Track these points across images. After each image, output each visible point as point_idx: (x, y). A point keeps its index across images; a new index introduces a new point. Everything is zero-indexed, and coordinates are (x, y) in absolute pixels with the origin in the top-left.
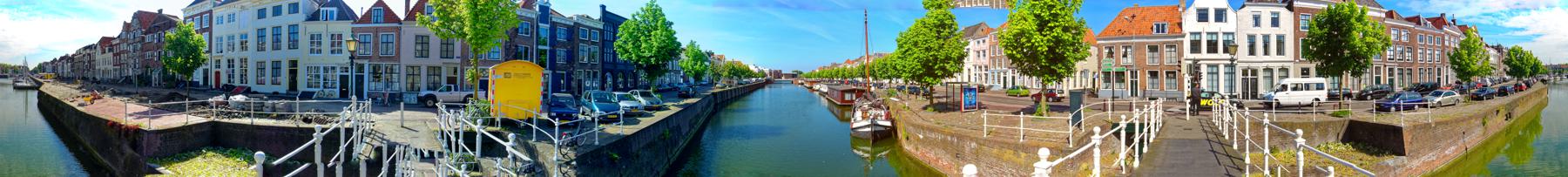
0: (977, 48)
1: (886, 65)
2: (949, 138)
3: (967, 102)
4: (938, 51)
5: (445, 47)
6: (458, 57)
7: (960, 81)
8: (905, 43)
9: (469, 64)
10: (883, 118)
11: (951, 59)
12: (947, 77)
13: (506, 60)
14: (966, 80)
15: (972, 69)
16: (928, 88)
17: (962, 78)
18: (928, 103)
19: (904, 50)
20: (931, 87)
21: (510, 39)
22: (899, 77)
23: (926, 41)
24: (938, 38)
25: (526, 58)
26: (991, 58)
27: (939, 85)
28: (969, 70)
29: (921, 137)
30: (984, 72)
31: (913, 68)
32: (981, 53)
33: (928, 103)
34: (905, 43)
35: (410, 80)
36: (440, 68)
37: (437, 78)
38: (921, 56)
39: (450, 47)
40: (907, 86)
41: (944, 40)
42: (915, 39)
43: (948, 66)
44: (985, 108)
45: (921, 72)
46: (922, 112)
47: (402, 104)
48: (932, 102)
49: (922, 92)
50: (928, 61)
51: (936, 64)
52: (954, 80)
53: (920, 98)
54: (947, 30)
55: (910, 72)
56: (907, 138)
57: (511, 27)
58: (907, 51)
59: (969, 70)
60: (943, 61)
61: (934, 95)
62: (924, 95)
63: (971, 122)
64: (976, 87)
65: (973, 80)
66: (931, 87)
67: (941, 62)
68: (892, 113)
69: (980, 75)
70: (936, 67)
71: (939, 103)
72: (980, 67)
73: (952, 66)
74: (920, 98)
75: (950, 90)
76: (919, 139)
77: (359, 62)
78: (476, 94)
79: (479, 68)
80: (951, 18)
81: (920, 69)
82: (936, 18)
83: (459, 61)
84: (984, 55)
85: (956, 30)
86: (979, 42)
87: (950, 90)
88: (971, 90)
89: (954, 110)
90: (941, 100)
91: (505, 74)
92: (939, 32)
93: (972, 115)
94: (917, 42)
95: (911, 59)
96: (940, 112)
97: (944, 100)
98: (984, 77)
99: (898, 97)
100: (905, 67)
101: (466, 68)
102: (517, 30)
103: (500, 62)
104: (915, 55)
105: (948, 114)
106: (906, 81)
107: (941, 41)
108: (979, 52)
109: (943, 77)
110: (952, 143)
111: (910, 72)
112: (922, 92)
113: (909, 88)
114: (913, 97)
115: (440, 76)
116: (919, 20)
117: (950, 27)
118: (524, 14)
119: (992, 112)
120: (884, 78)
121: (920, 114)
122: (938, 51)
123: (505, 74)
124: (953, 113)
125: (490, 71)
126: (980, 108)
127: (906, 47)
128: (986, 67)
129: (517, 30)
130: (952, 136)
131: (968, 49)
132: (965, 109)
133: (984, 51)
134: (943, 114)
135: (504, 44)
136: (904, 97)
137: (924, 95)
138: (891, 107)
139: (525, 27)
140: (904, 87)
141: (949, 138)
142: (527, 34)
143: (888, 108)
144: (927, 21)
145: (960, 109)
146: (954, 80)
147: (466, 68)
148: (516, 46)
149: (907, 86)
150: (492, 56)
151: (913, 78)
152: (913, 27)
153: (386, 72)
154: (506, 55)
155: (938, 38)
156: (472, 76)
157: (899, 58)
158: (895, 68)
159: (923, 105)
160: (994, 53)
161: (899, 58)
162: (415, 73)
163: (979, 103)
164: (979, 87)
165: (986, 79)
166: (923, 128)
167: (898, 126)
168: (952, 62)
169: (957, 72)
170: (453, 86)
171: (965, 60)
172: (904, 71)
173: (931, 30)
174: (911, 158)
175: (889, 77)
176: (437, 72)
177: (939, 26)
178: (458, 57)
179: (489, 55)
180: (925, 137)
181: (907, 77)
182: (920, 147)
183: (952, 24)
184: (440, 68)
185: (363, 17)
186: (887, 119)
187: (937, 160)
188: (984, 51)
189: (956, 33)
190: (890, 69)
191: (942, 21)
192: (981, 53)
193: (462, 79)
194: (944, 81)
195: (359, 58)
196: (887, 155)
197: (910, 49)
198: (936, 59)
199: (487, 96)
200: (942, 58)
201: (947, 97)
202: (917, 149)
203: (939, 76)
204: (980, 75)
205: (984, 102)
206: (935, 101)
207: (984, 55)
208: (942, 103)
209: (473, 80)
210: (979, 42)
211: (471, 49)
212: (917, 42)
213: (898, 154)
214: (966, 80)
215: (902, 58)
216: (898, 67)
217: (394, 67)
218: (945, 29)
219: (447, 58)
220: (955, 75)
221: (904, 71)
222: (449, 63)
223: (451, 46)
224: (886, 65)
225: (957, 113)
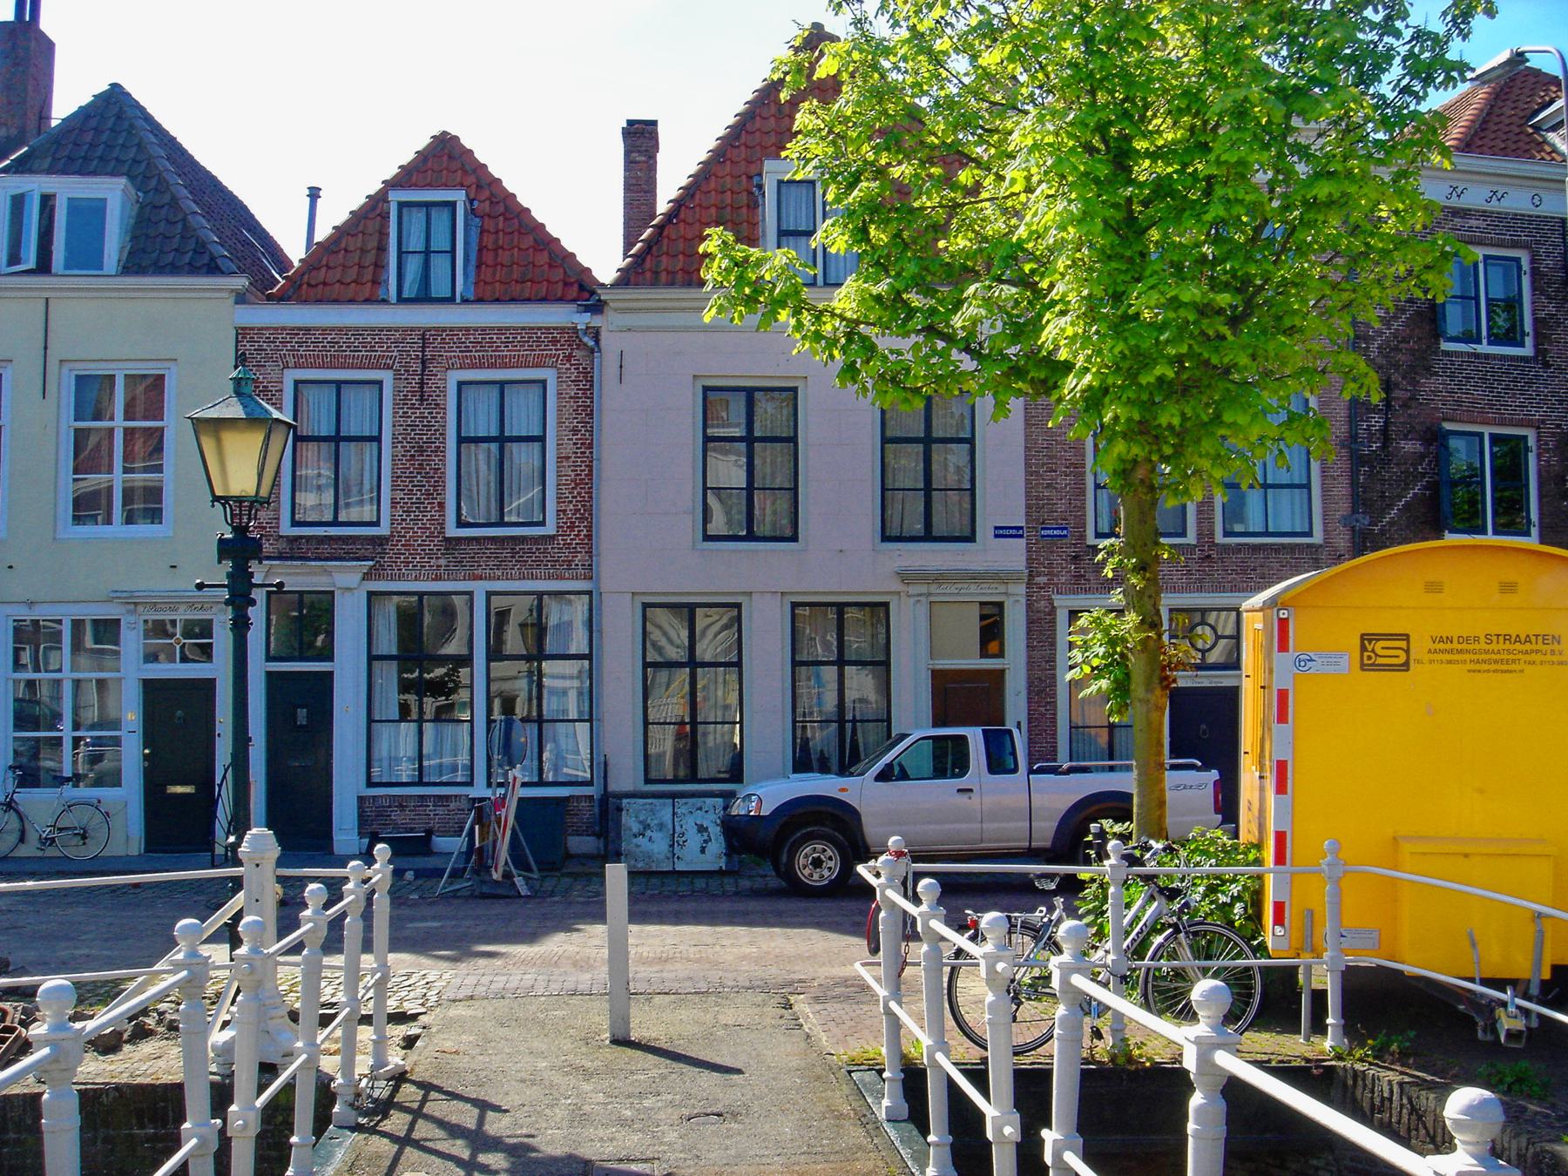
5: (908, 462)
6: (1001, 532)
9: (1085, 575)
13: (1363, 542)
21: (1387, 386)
25: (1511, 518)
35: (671, 705)
36: (879, 610)
37: (860, 684)
39: (950, 461)
47: (616, 876)
57: (1391, 294)
77: (300, 578)
78: (1151, 782)
79: (1168, 601)
83: (1013, 555)
91: (1366, 639)
101: (1063, 603)
102: (1430, 317)
103: (1311, 557)
115: (881, 665)
118: (1475, 198)
123: (1366, 639)
125: (1254, 625)
129: (1430, 317)
135: (1342, 429)
139: (1490, 286)
142: (1511, 336)
147: (1063, 603)
148: (1436, 438)
150: (1254, 521)
153: (495, 653)
154: (1360, 500)
156: (1117, 663)
162: (705, 651)
170: (975, 736)
176: (857, 642)
178: (1001, 532)
179: (1234, 512)
184: (879, 610)
185: (323, 254)
193: (1042, 687)
195: (295, 550)
199: (1227, 805)
209: (1122, 688)
211: (1100, 467)
217: (554, 614)
219: (928, 536)
222: (939, 578)
223: (958, 454)
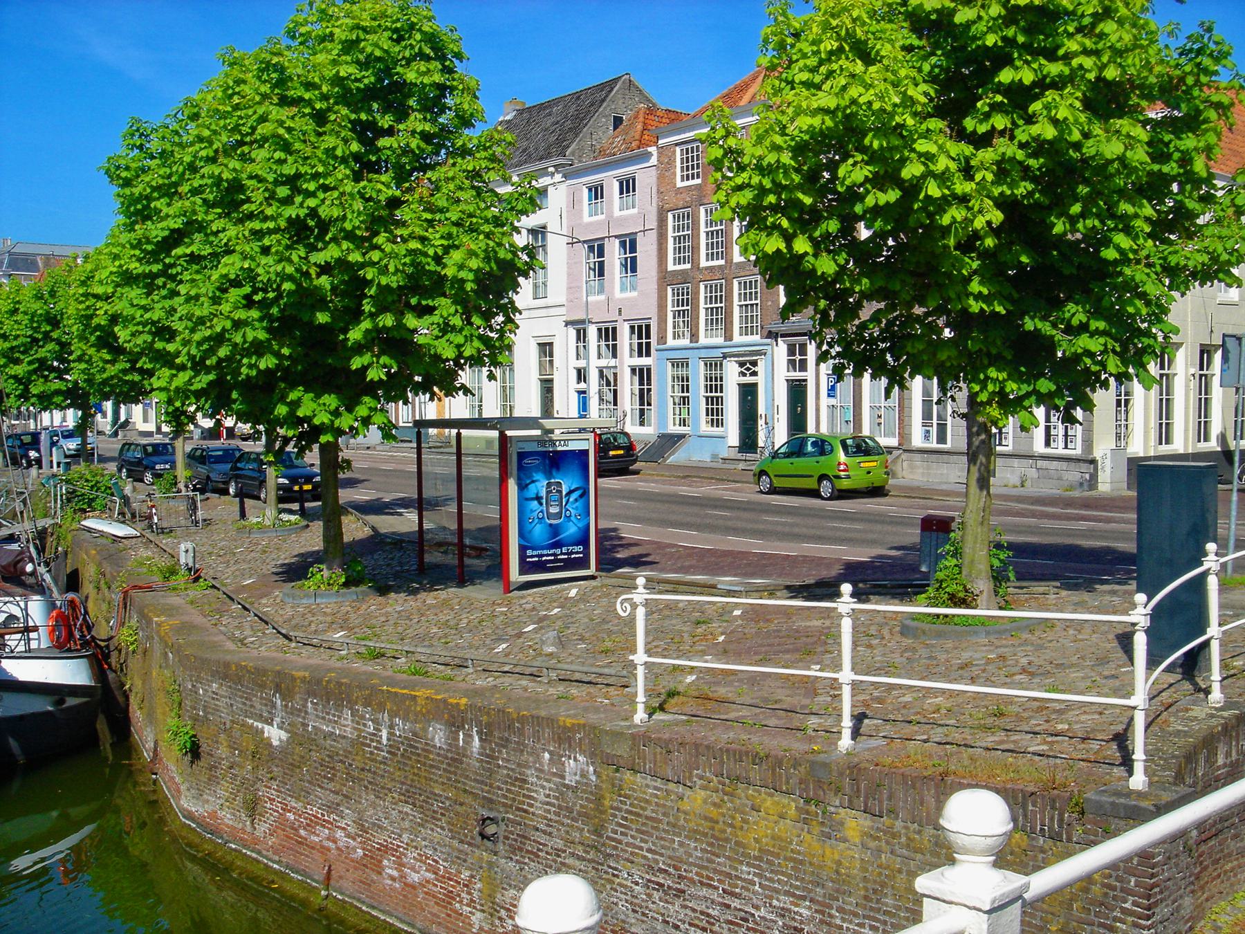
0: (591, 221)
1: (54, 322)
2: (438, 735)
3: (539, 532)
4: (363, 242)
7: (492, 410)
8: (169, 191)
10: (40, 640)
11: (438, 285)
12: (425, 387)
14: (527, 404)
15: (565, 342)
16: (313, 457)
17: (506, 394)
18: (313, 539)
19: (157, 231)
20: (329, 452)
22: (133, 393)
23: (293, 181)
24: (365, 167)
26: (665, 279)
27: (374, 435)
28: (546, 349)
29: (275, 734)
30: (628, 360)
31: (219, 339)
32: (614, 255)
33: (313, 539)
34: (169, 191)
38: (267, 267)
40: (182, 448)
41: (401, 176)
42: (229, 169)
43: (423, 330)
44: (637, 562)
45: (267, 362)
46: (280, 592)
48: (333, 533)
49: (274, 477)
50: (308, 298)
51: (355, 315)
52: (458, 407)
53: (264, 513)
54: (417, 122)
55: (198, 366)
56: (194, 752)
58: (176, 238)
59: (546, 349)
60: (392, 300)
61: (345, 495)
62: (286, 496)
63: (561, 642)
64: (586, 444)
65: (566, 403)
66: (329, 452)
67: (382, 309)
68: (95, 610)
69: (609, 381)
70: (355, 335)
71: (377, 541)
72: (608, 334)
73: (446, 328)
74: (264, 513)
75: (439, 466)
76: (261, 751)
80: (437, 50)
81: (258, 349)
82: (350, 46)
84: (631, 266)
85: (466, 121)
86: (597, 192)
87: (439, 466)
88: (555, 461)
89: (463, 578)
90: (387, 524)
92: (367, 132)
93: (565, 603)
94: (236, 186)
95: (207, 289)
96: (383, 590)
97: (407, 522)
98: (628, 387)
99: (127, 515)
100: (165, 333)
104: (231, 266)
105: (430, 598)
106: (179, 419)
107: (383, 186)
108: (595, 247)
109: (396, 388)
110: (456, 758)
111: (198, 366)
112: (274, 477)
113: (198, 458)
114: (224, 507)
116: (250, 53)
117: (433, 103)
119: (676, 587)
120: (46, 402)
121: (266, 606)
122: (363, 242)
124: (452, 593)
126: (608, 564)
127: (171, 215)
128: (641, 331)
130: (455, 721)
131: (539, 232)
132: (525, 567)
133: (629, 243)
134: (398, 602)
136: (170, 510)
137: (286, 496)
138: (89, 573)
140: (162, 451)
141: (438, 735)
143: (73, 582)
144: (294, 61)
145: (498, 570)
146: (458, 407)
149: (182, 448)
151: (217, 396)
152: (210, 99)
155: (365, 167)
157: (128, 279)
158: (107, 341)
159: (286, 556)
160: (688, 249)
161: (128, 279)
163: (603, 535)
164: (603, 445)
165: (644, 398)
166: (283, 684)
167: (134, 682)
168: (445, 307)
169: (476, 361)
171: (523, 296)
172: (167, 360)
173: (320, 118)
174: (216, 866)
175: (76, 397)
177: (370, 94)
180: (298, 737)
181: (183, 393)
182: (269, 792)
183: (442, 89)
186: (62, 647)
187: (373, 861)
188: (629, 243)
189: (470, 137)
190: (77, 347)
191: (384, 65)
192: (614, 255)
194: (402, 414)
196: (77, 861)
197: (192, 227)
198: (354, 285)
200: (393, 281)
201: (421, 504)
202: (253, 808)
203: (371, 389)
204: (609, 381)
205: (630, 531)
206: (354, 529)
207: (631, 266)
208: (398, 542)
210: (597, 192)
212: (236, 186)
213: (138, 846)
214: (527, 404)
215: (149, 283)
216: (122, 334)
218: (402, 114)
220: (465, 377)
221: (167, 360)
224: (54, 322)
225: (482, 594)
